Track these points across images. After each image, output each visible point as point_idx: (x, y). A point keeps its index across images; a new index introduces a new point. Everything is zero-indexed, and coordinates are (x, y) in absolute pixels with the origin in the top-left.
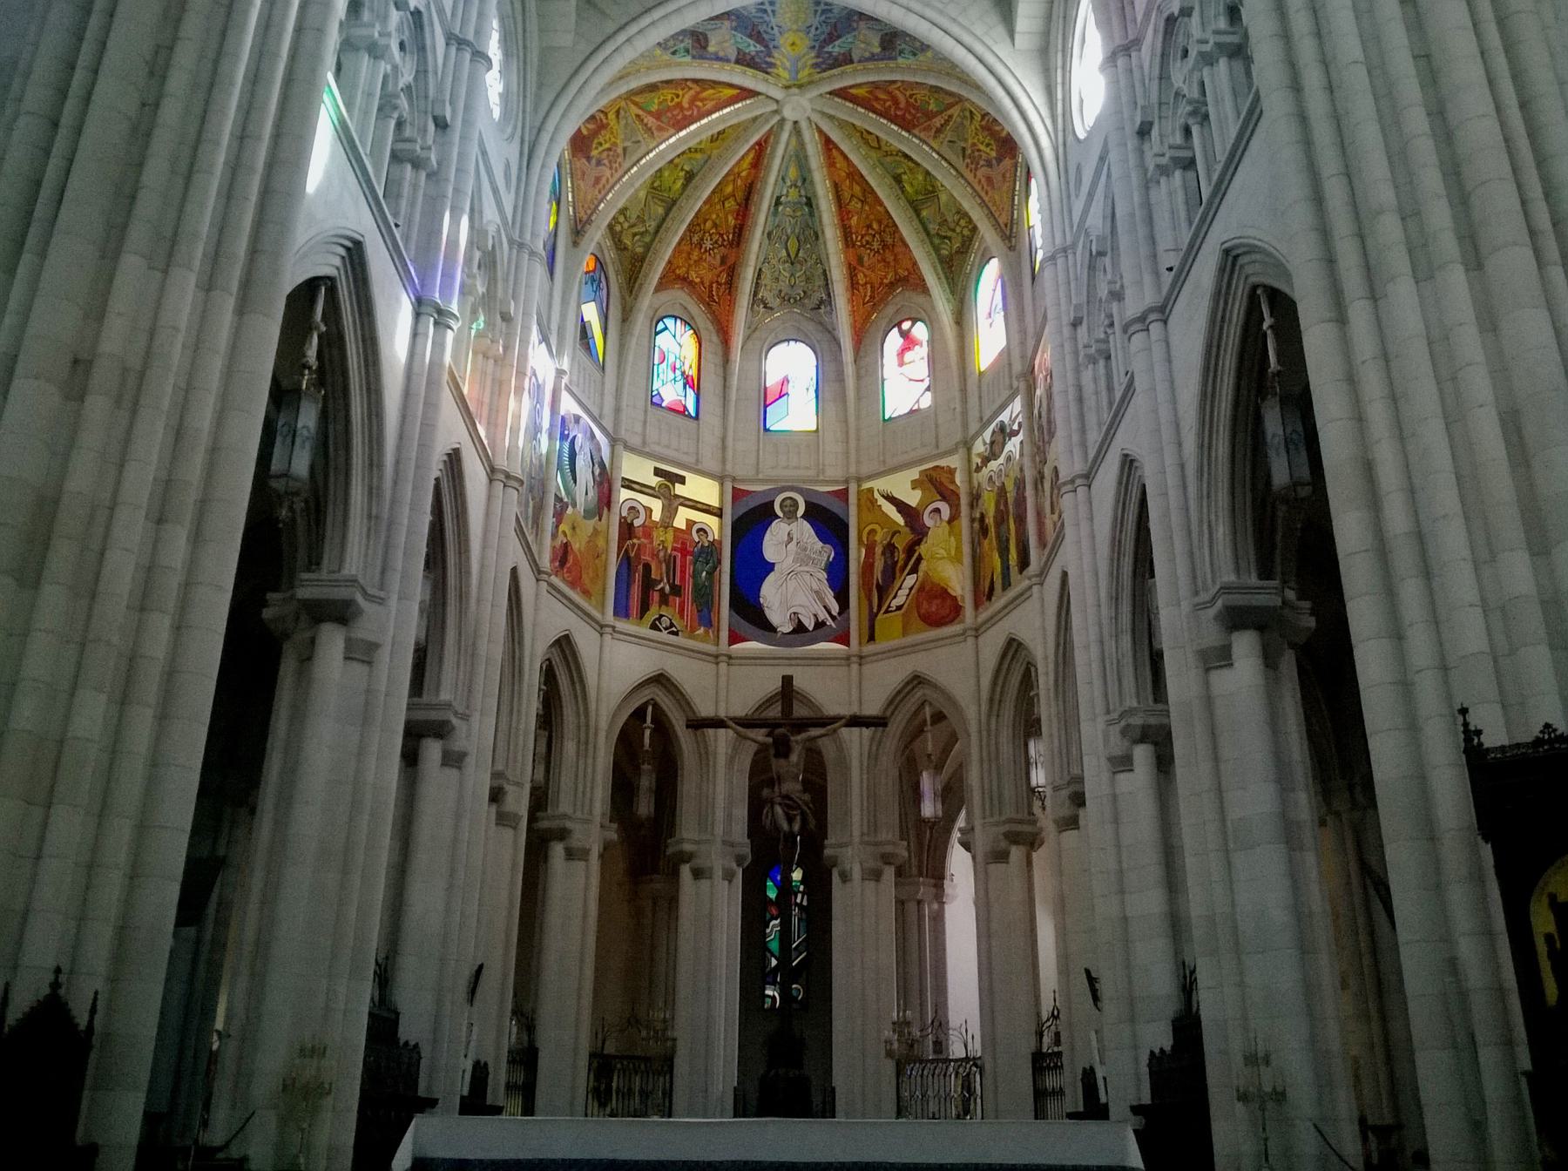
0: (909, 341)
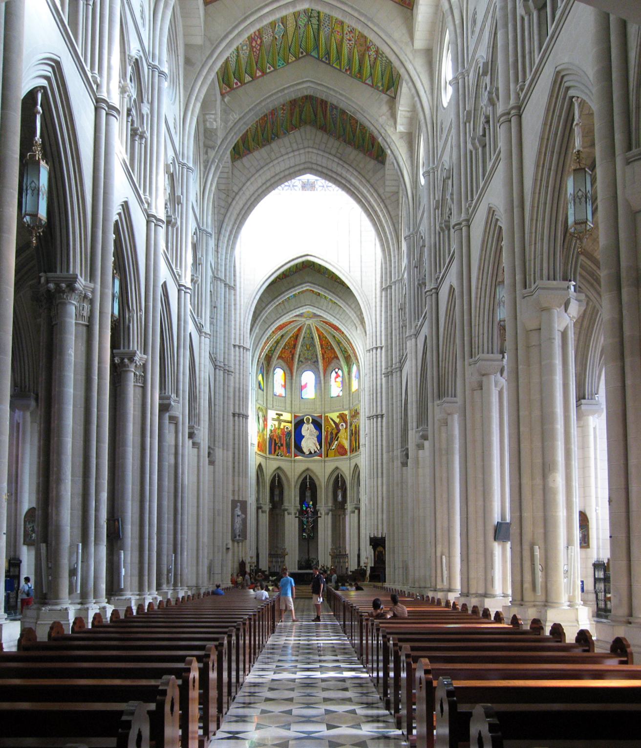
0: (338, 376)
